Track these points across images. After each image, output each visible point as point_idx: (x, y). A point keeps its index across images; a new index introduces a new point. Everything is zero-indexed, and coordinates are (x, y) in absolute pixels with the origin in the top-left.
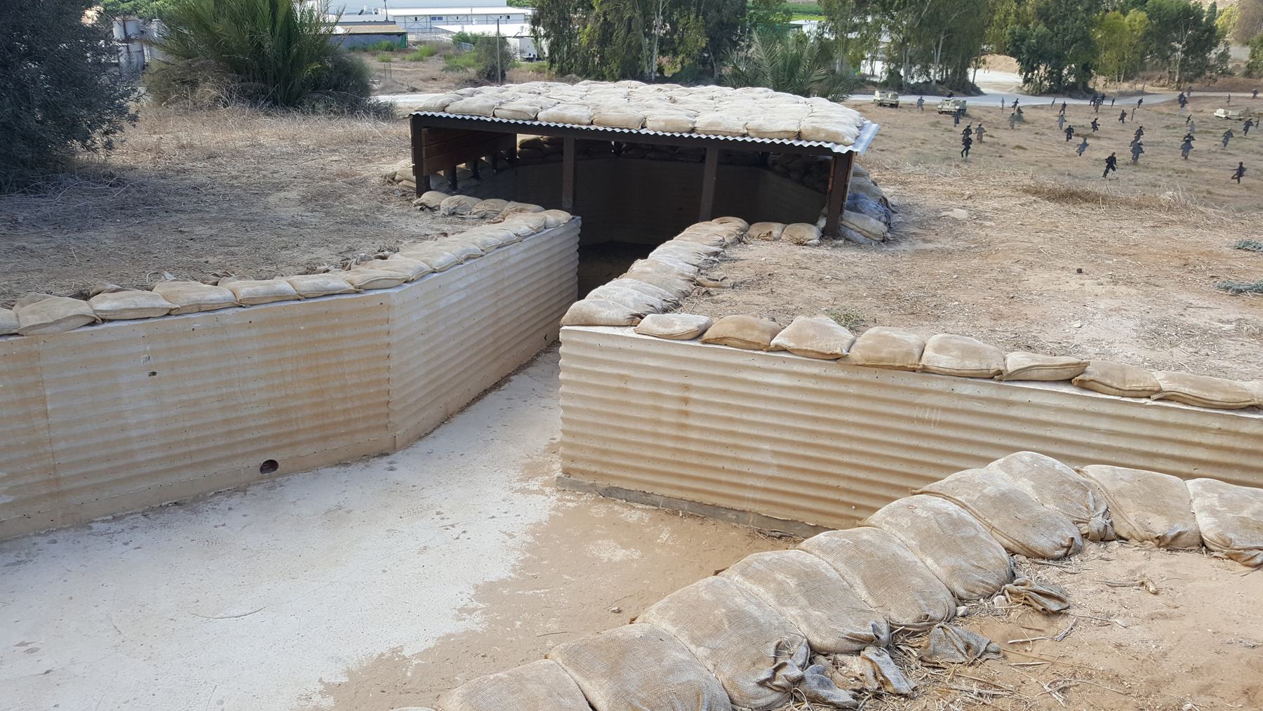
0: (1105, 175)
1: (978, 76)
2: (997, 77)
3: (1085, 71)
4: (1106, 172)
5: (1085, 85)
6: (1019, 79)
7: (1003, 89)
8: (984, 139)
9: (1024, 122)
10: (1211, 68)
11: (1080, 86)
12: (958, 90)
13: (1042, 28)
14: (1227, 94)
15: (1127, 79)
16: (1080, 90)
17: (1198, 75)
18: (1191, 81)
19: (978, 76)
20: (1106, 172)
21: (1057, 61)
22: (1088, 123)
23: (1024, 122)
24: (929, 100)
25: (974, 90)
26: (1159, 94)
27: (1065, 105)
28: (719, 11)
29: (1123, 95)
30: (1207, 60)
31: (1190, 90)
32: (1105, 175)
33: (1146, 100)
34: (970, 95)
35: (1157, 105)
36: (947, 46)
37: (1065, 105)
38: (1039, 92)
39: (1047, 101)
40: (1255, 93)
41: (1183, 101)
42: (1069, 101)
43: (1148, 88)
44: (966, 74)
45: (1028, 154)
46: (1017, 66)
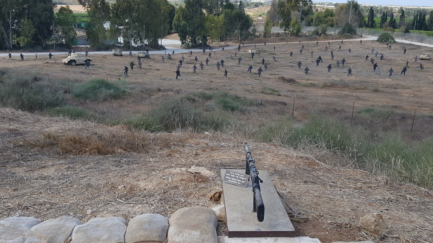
0: (177, 78)
1: (163, 42)
2: (171, 43)
3: (204, 38)
4: (177, 77)
5: (205, 44)
6: (179, 42)
7: (176, 47)
8: (143, 66)
9: (172, 59)
11: (203, 44)
12: (155, 48)
13: (183, 22)
14: (254, 45)
15: (222, 40)
16: (204, 46)
17: (246, 38)
18: (245, 40)
19: (163, 42)
20: (177, 77)
21: (193, 35)
22: (194, 58)
23: (172, 59)
24: (134, 52)
25: (162, 48)
26: (233, 46)
27: (191, 52)
28: (40, 17)
29: (220, 46)
30: (249, 32)
31: (243, 44)
32: (177, 78)
33: (225, 48)
34: (160, 50)
35: (232, 50)
36: (147, 30)
37: (191, 52)
38: (188, 47)
39: (187, 51)
40: (265, 43)
41: (239, 48)
42: (193, 50)
43: (230, 43)
44: (157, 41)
45: (160, 71)
46: (179, 38)
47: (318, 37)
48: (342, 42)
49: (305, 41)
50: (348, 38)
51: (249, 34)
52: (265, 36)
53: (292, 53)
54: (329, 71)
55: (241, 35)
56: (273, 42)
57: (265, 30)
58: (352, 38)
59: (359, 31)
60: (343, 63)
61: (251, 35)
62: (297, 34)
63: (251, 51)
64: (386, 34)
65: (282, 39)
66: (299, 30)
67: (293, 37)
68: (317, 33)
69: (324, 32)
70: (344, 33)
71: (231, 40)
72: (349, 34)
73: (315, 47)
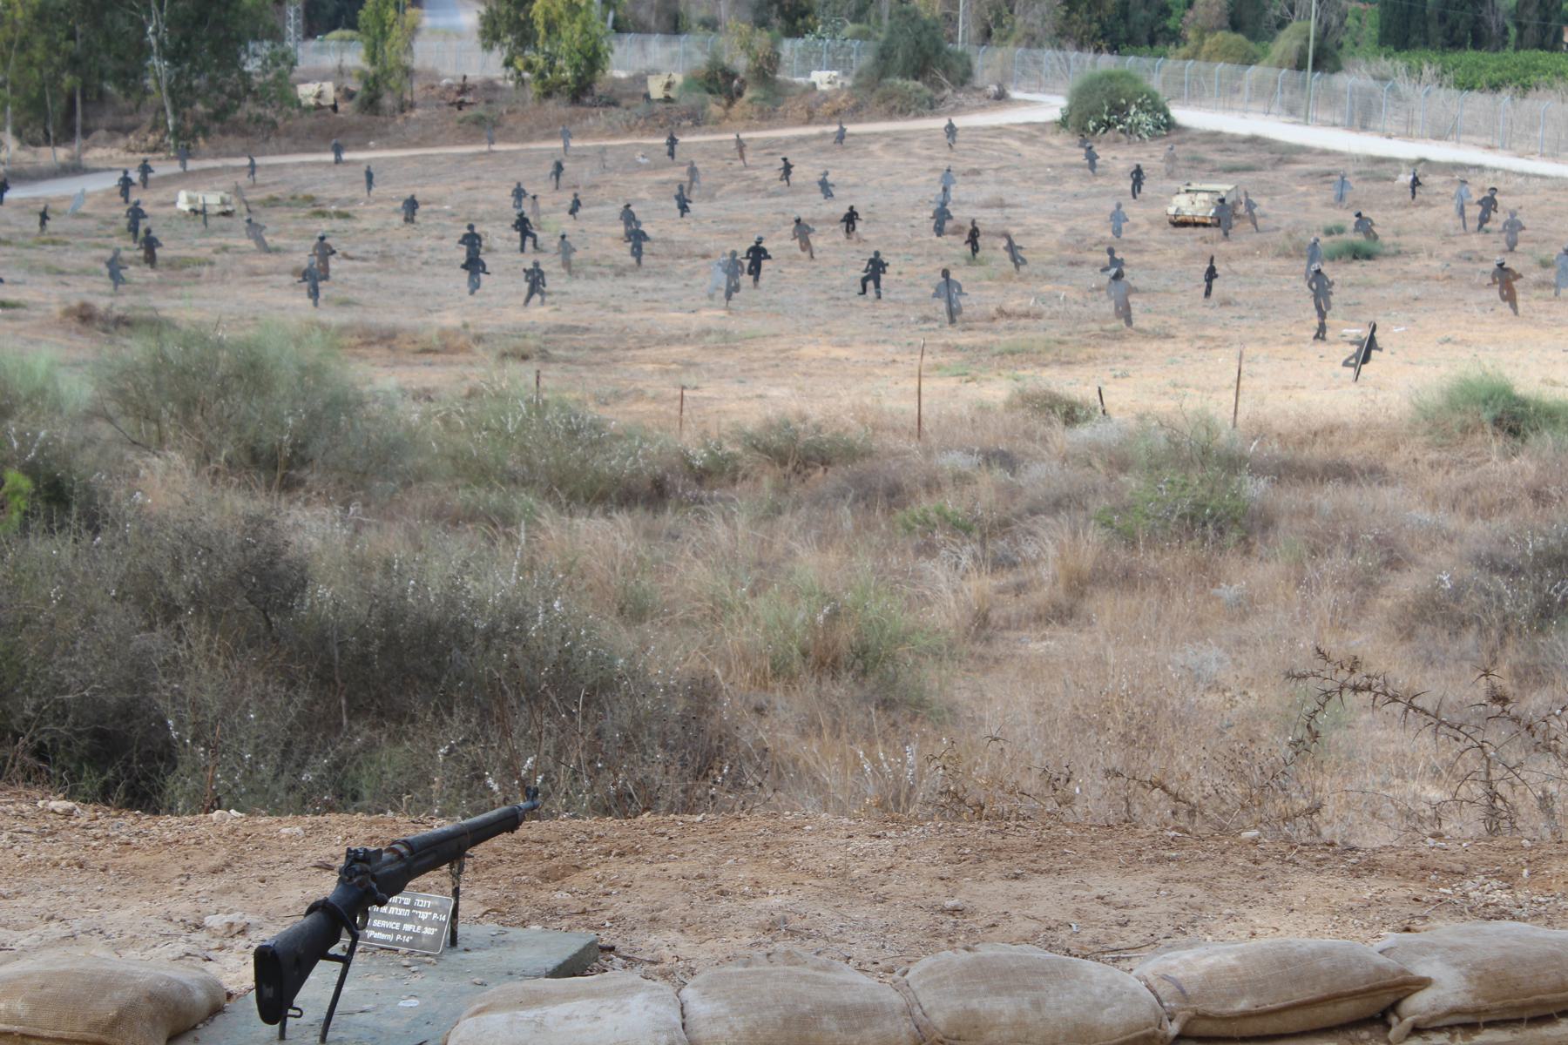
10: (258, 96)
47: (715, 109)
48: (841, 136)
49: (630, 130)
50: (904, 113)
51: (246, 89)
52: (371, 104)
53: (411, 205)
54: (475, 286)
55: (181, 97)
56: (418, 145)
57: (373, 59)
58: (932, 106)
59: (987, 64)
60: (755, 270)
61: (258, 96)
62: (582, 88)
63: (190, 200)
64: (1111, 77)
65: (479, 121)
66: (593, 60)
67: (557, 108)
68: (719, 82)
69: (766, 72)
70: (884, 74)
71: (126, 131)
72: (912, 84)
73: (656, 167)
